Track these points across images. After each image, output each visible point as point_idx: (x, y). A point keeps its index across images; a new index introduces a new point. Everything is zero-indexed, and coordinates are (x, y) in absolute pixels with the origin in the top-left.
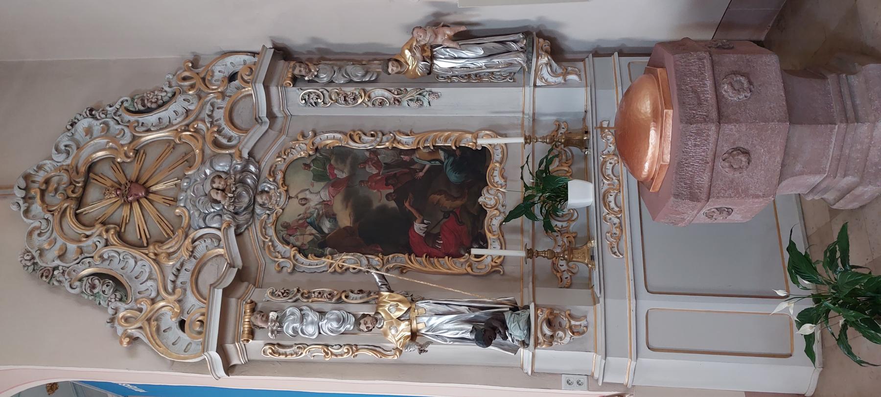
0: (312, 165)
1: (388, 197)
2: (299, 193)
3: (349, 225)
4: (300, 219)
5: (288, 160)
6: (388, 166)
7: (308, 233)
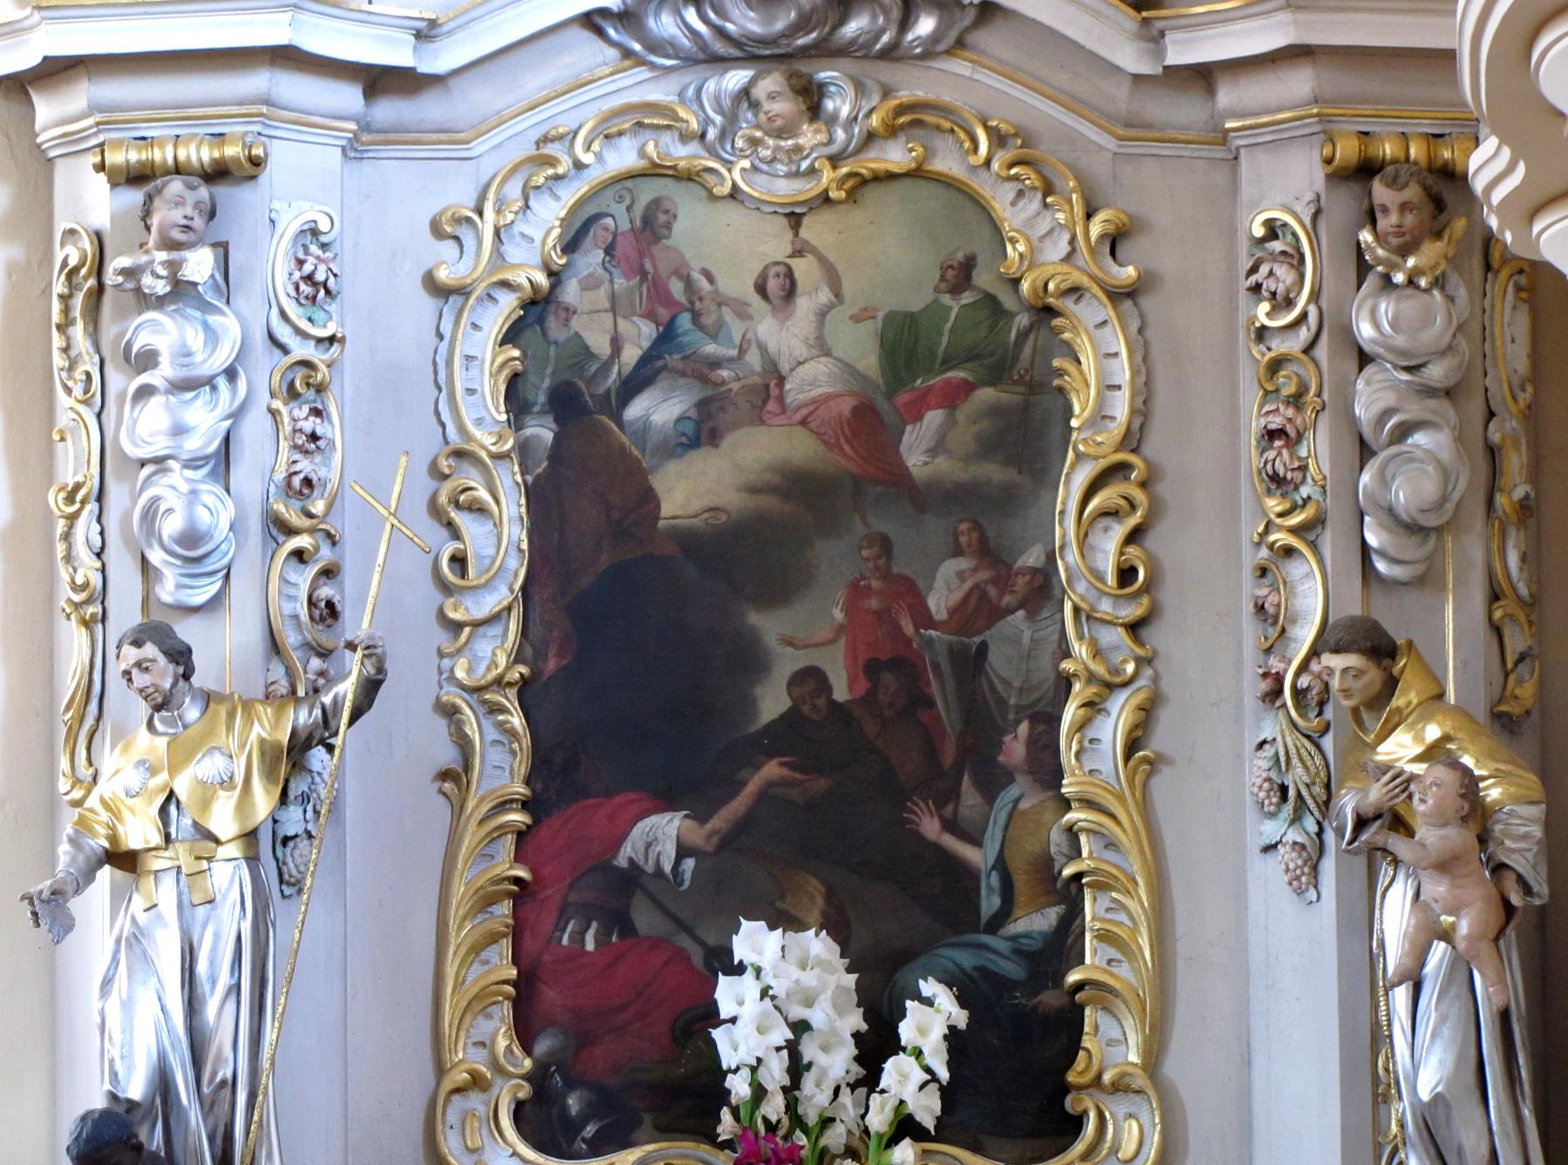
0: (967, 298)
1: (811, 679)
2: (821, 259)
3: (667, 509)
4: (689, 283)
5: (983, 186)
6: (971, 663)
7: (623, 325)
